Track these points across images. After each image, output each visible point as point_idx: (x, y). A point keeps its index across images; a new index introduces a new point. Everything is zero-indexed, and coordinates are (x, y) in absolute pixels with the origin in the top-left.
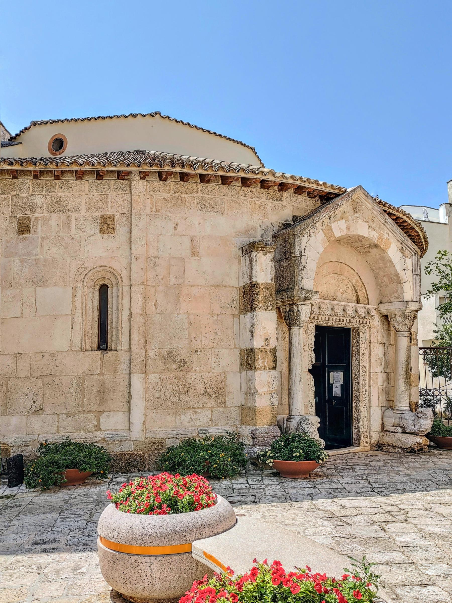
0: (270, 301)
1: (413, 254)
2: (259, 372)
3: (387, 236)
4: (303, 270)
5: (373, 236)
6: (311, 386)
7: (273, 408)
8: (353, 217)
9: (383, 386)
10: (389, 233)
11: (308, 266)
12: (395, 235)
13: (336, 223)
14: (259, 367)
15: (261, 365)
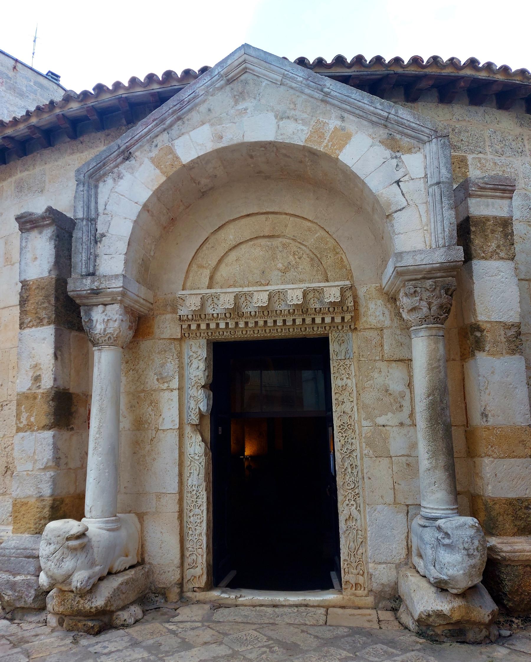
0: (45, 308)
1: (426, 138)
2: (21, 434)
3: (338, 123)
4: (100, 242)
5: (295, 133)
6: (197, 457)
7: (43, 500)
8: (232, 112)
9: (408, 456)
10: (346, 115)
11: (112, 230)
12: (361, 113)
13: (186, 137)
14: (21, 425)
15: (25, 422)
